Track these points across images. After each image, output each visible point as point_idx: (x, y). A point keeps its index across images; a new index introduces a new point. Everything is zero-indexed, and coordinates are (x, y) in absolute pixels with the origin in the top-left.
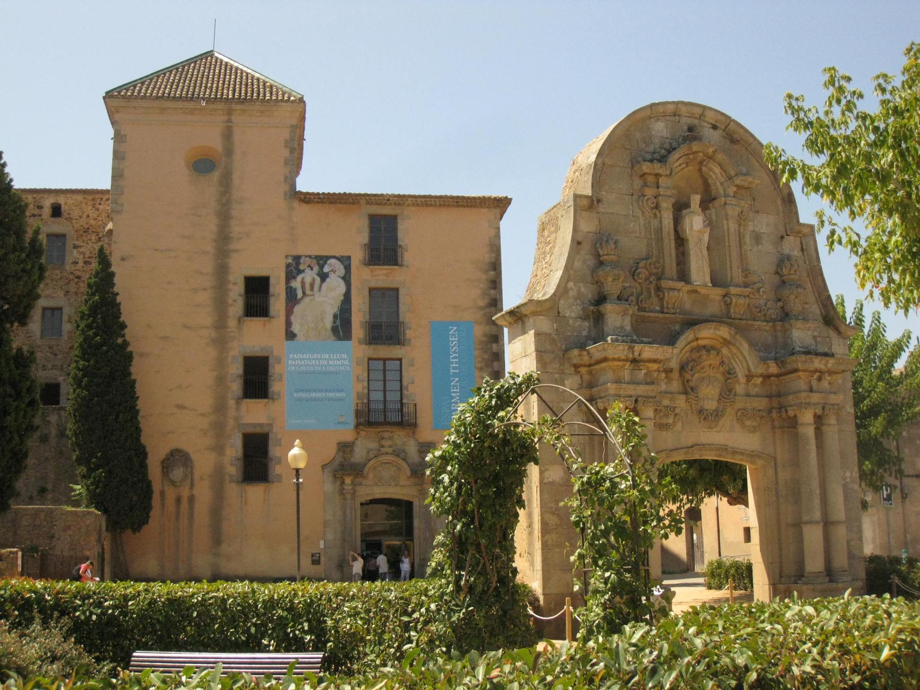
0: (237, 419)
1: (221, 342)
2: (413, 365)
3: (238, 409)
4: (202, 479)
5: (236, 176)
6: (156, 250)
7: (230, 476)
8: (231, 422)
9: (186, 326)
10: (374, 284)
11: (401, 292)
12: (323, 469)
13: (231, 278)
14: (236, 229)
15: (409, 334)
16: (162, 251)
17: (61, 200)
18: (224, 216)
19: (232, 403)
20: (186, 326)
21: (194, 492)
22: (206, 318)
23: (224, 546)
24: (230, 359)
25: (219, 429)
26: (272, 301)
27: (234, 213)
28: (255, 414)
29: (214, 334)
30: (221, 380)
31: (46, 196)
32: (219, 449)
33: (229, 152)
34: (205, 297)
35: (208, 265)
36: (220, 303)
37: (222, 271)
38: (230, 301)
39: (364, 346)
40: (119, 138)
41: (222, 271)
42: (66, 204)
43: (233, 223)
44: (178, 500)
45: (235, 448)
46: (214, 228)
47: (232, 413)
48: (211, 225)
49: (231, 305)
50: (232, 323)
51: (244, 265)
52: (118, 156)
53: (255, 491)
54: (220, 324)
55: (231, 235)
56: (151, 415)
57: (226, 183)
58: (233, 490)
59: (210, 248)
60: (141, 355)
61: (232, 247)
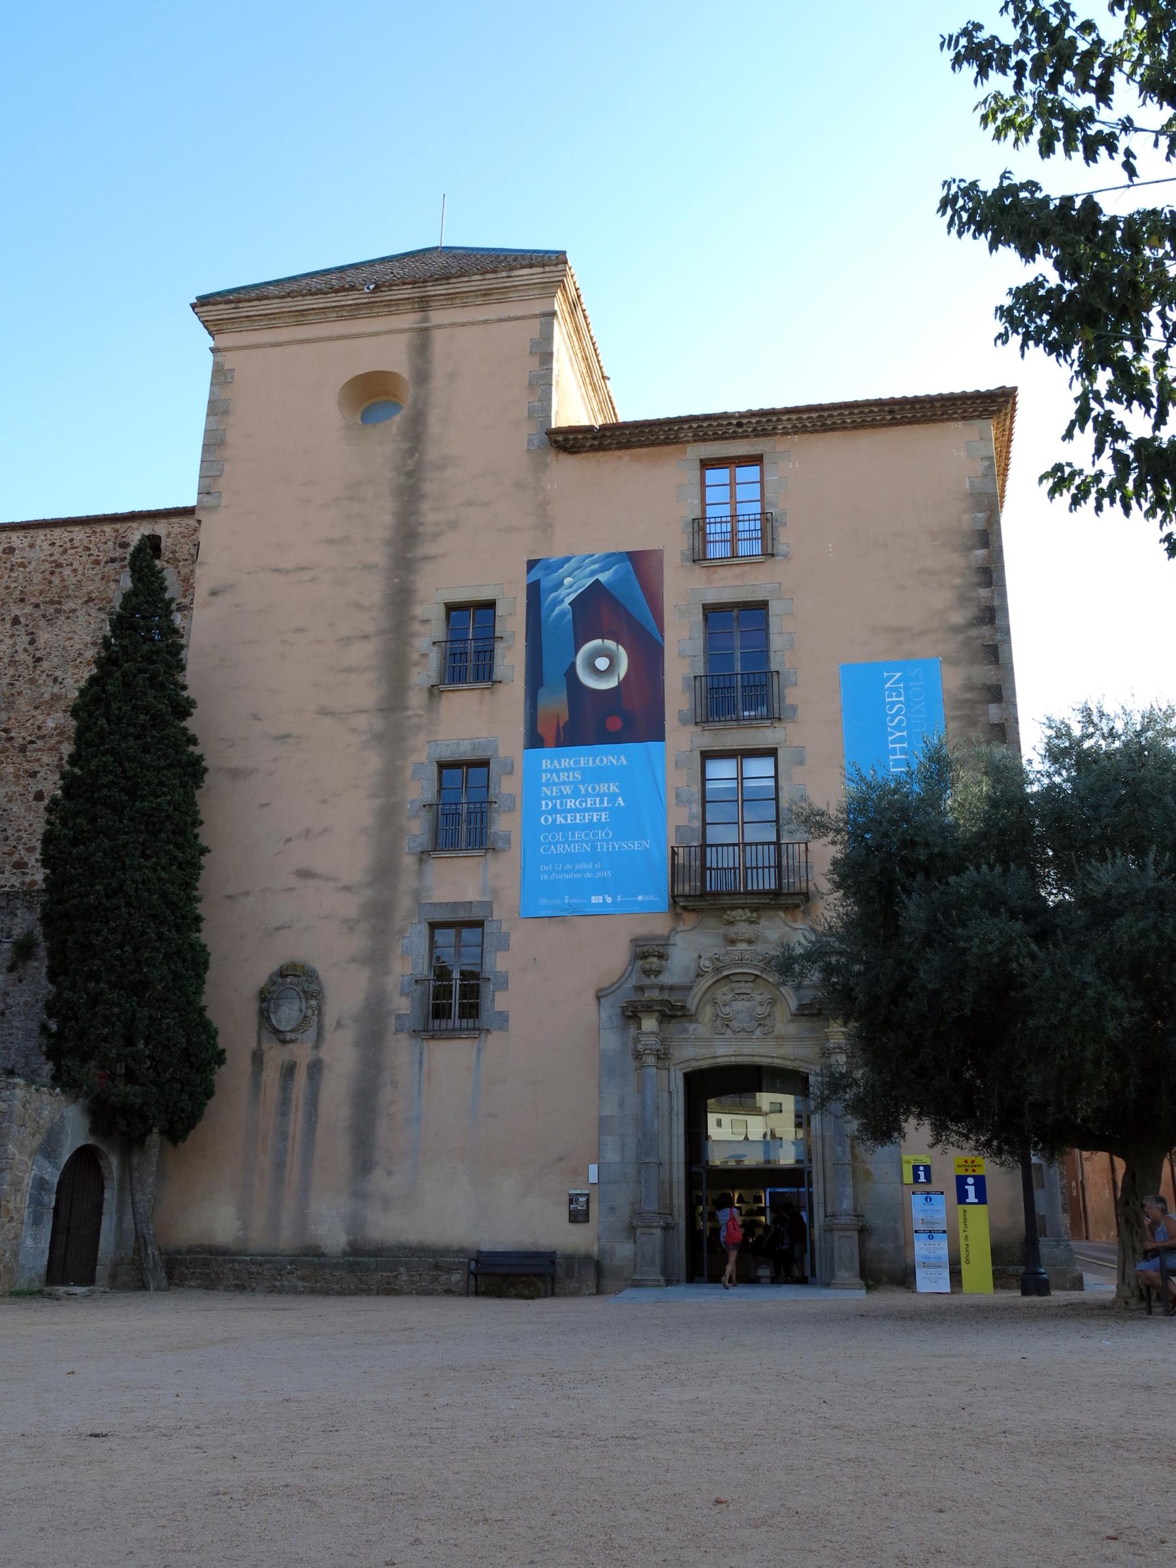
0: (417, 895)
1: (392, 737)
2: (801, 762)
3: (420, 873)
4: (339, 1025)
5: (434, 416)
6: (278, 571)
7: (399, 1017)
8: (405, 903)
9: (324, 712)
10: (712, 597)
11: (773, 608)
12: (598, 998)
13: (419, 611)
14: (430, 516)
15: (791, 696)
16: (287, 572)
17: (161, 528)
18: (410, 492)
19: (408, 861)
20: (324, 712)
21: (321, 1055)
22: (365, 692)
23: (378, 1175)
24: (409, 772)
25: (380, 915)
26: (499, 648)
27: (428, 487)
28: (456, 882)
29: (379, 724)
30: (388, 816)
31: (135, 525)
32: (376, 959)
33: (422, 377)
34: (364, 652)
35: (373, 591)
36: (395, 665)
37: (401, 598)
38: (415, 657)
39: (692, 728)
40: (221, 376)
41: (401, 598)
42: (168, 536)
43: (425, 506)
44: (289, 1070)
45: (410, 960)
46: (388, 519)
47: (407, 881)
48: (382, 514)
49: (417, 664)
50: (416, 700)
51: (445, 581)
52: (217, 409)
53: (451, 1056)
54: (393, 702)
55: (422, 529)
56: (247, 894)
57: (416, 433)
58: (401, 1051)
59: (379, 557)
60: (236, 774)
61: (420, 551)
